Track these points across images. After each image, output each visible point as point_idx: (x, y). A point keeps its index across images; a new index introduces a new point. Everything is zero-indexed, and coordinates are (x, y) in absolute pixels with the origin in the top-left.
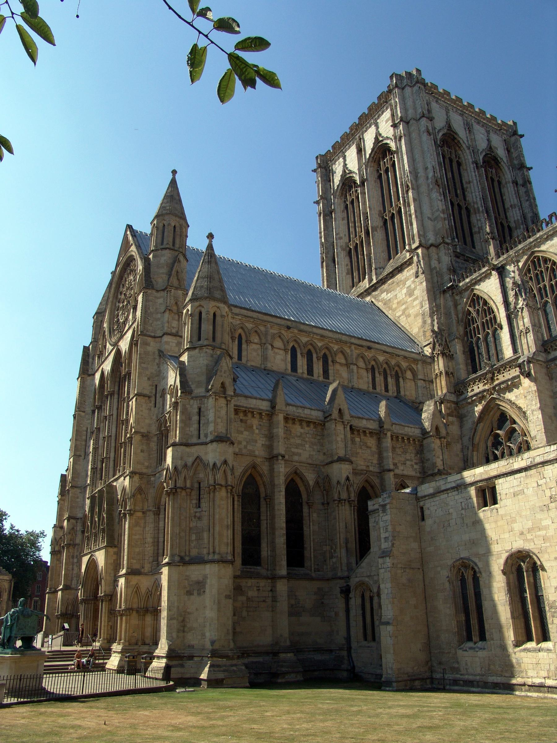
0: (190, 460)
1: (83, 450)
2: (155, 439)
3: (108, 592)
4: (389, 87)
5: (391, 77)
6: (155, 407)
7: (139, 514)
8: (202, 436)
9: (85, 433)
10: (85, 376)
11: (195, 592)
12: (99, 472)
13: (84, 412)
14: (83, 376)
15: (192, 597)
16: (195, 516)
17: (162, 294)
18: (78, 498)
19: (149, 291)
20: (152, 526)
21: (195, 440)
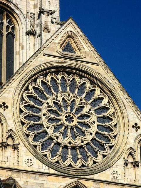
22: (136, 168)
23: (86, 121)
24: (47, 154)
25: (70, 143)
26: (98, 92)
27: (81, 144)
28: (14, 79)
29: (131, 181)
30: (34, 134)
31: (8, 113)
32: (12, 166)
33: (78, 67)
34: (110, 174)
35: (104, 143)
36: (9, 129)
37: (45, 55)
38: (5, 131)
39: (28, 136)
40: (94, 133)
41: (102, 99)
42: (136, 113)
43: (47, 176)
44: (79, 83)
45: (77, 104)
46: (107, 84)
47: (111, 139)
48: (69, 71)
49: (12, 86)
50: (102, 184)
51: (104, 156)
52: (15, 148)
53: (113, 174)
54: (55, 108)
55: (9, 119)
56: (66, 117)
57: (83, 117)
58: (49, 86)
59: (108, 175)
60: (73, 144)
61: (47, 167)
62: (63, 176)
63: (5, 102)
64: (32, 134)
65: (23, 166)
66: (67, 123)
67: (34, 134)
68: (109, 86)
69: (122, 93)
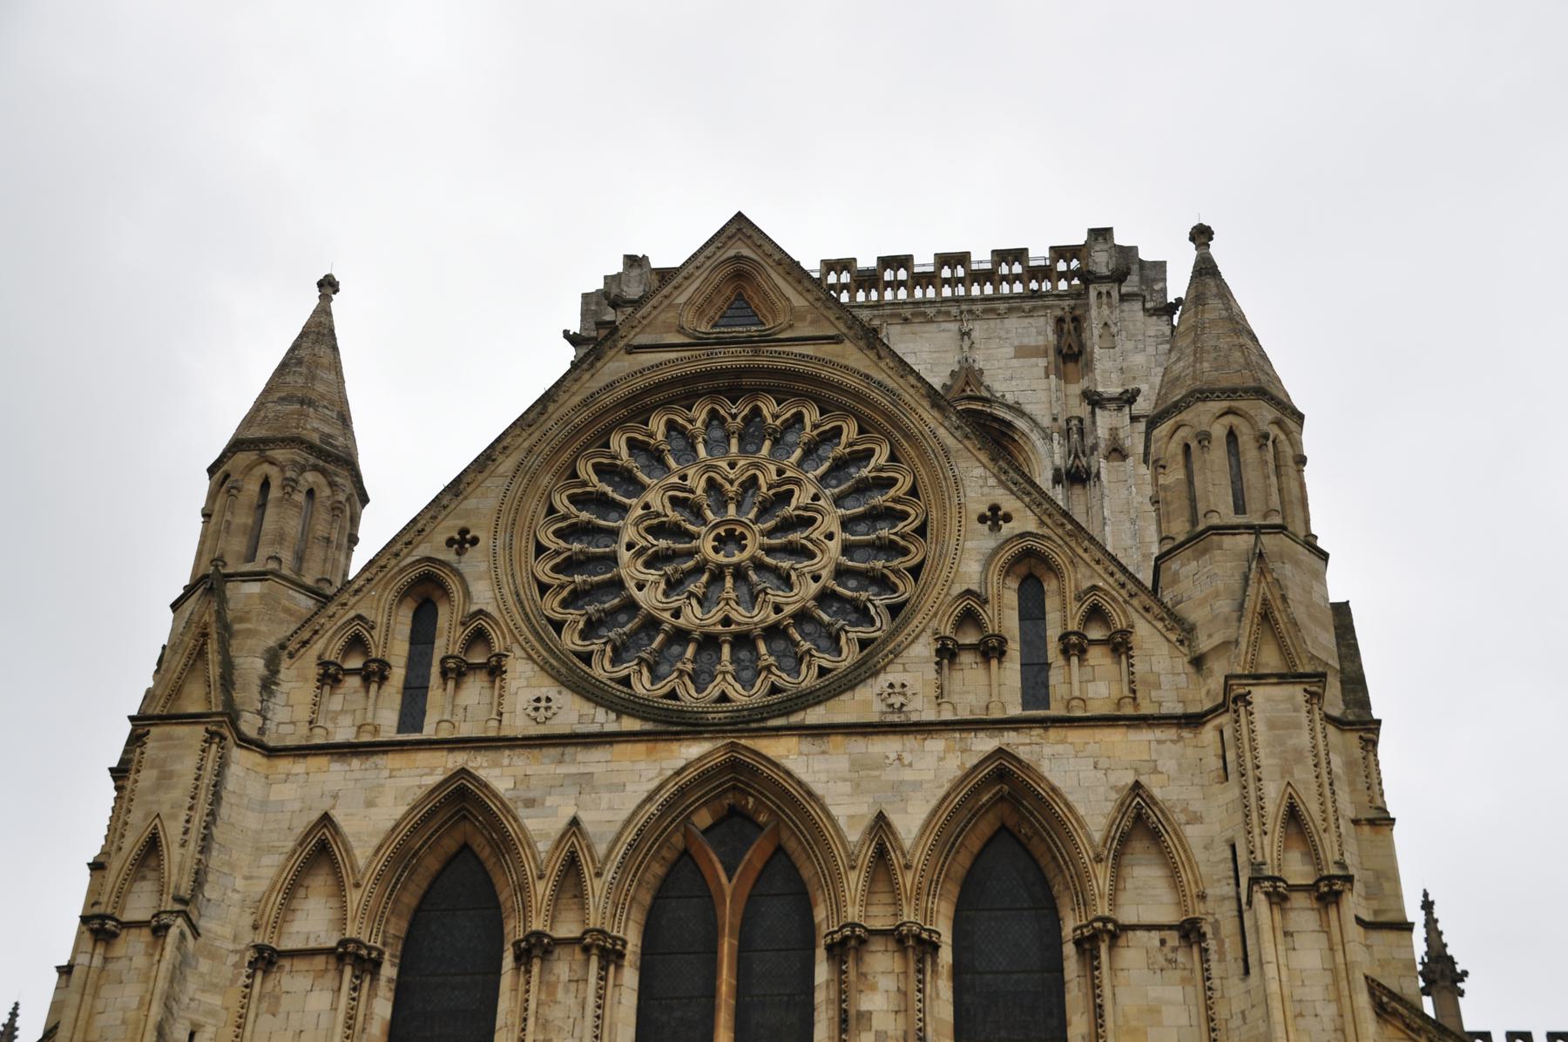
4: (1059, 252)
5: (1101, 235)
14: (226, 732)
22: (994, 663)
23: (796, 536)
24: (629, 675)
25: (727, 621)
26: (850, 430)
27: (773, 617)
28: (505, 448)
29: (971, 711)
30: (584, 618)
31: (474, 564)
32: (476, 732)
33: (763, 362)
34: (875, 697)
35: (870, 601)
36: (474, 608)
37: (632, 350)
38: (458, 617)
39: (558, 626)
41: (869, 454)
42: (996, 471)
43: (607, 746)
44: (775, 417)
45: (764, 489)
46: (876, 395)
47: (897, 581)
48: (732, 385)
49: (501, 469)
50: (839, 739)
51: (864, 644)
52: (495, 670)
53: (885, 695)
54: (674, 515)
55: (480, 578)
56: (714, 540)
57: (787, 525)
58: (657, 449)
59: (867, 703)
60: (738, 624)
61: (613, 716)
62: (676, 736)
63: (468, 525)
64: (575, 618)
65: (518, 724)
66: (721, 558)
67: (583, 615)
68: (885, 402)
69: (936, 414)
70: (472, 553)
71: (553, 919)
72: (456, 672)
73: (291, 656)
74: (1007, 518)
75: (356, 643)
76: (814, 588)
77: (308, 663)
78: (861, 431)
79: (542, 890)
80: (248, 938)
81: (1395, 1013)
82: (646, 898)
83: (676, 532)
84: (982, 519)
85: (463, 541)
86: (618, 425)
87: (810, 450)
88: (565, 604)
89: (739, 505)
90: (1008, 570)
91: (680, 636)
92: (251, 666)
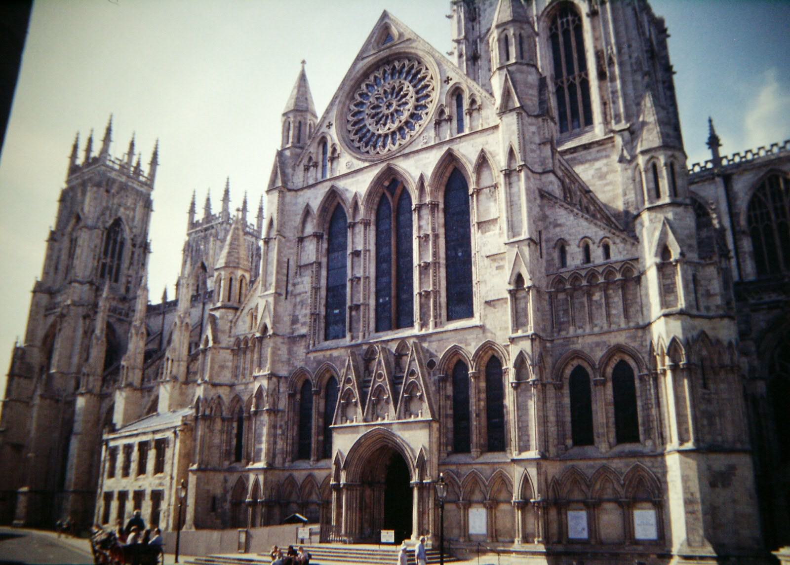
0: (695, 333)
1: (284, 288)
2: (547, 297)
3: (434, 479)
6: (541, 257)
7: (539, 386)
8: (702, 308)
9: (286, 265)
10: (285, 190)
11: (720, 485)
12: (323, 321)
13: (285, 237)
14: (283, 189)
15: (717, 490)
16: (704, 399)
17: (533, 120)
18: (279, 350)
19: (524, 114)
20: (554, 401)
21: (694, 312)
23: (404, 100)
25: (389, 129)
26: (416, 64)
33: (392, 52)
37: (363, 59)
40: (411, 109)
48: (387, 61)
70: (333, 128)
71: (354, 217)
72: (333, 159)
73: (298, 166)
74: (451, 79)
75: (310, 159)
76: (409, 112)
77: (302, 167)
78: (419, 63)
79: (351, 211)
80: (297, 235)
81: (545, 196)
82: (375, 207)
83: (378, 107)
84: (445, 82)
85: (329, 126)
86: (363, 81)
87: (408, 73)
88: (356, 134)
89: (392, 95)
90: (452, 94)
91: (380, 136)
92: (289, 171)
